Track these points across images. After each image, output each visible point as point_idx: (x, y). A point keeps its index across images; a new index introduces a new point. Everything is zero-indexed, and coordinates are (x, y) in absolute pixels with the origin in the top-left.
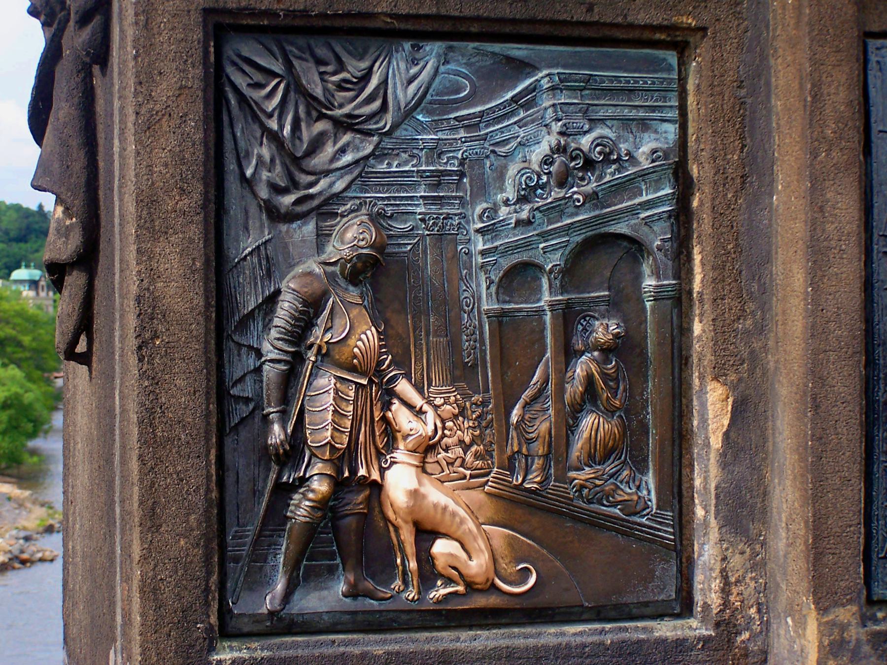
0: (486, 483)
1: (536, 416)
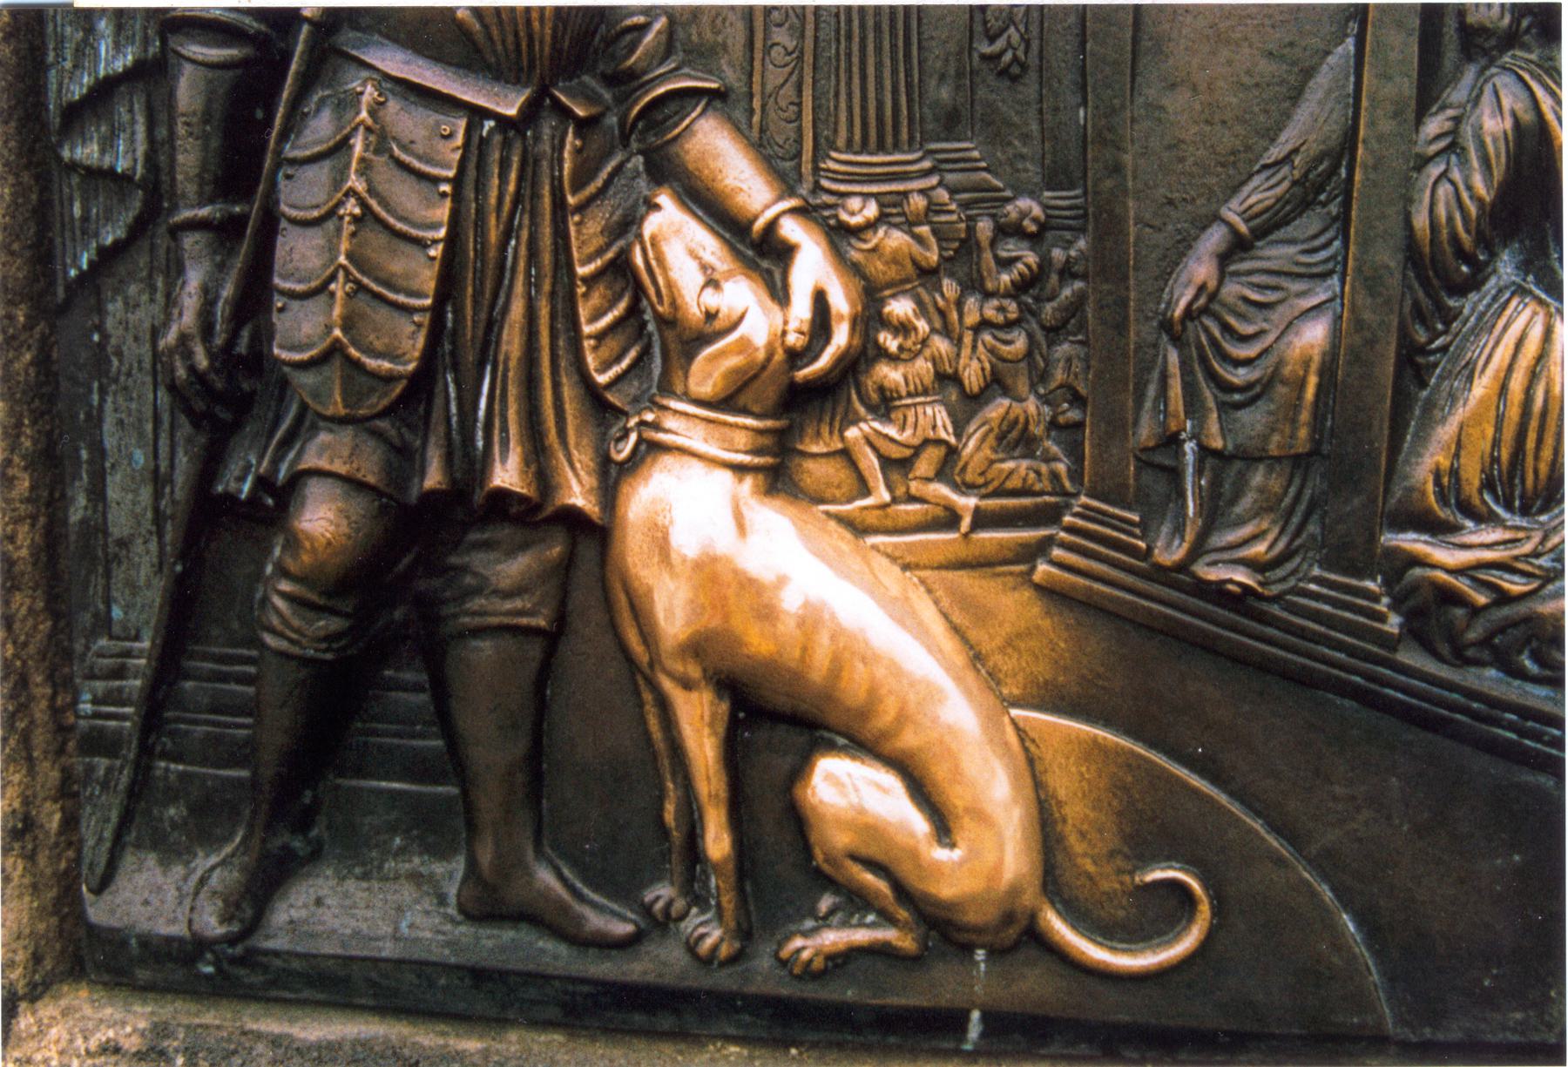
0: (1041, 549)
1: (1271, 297)
